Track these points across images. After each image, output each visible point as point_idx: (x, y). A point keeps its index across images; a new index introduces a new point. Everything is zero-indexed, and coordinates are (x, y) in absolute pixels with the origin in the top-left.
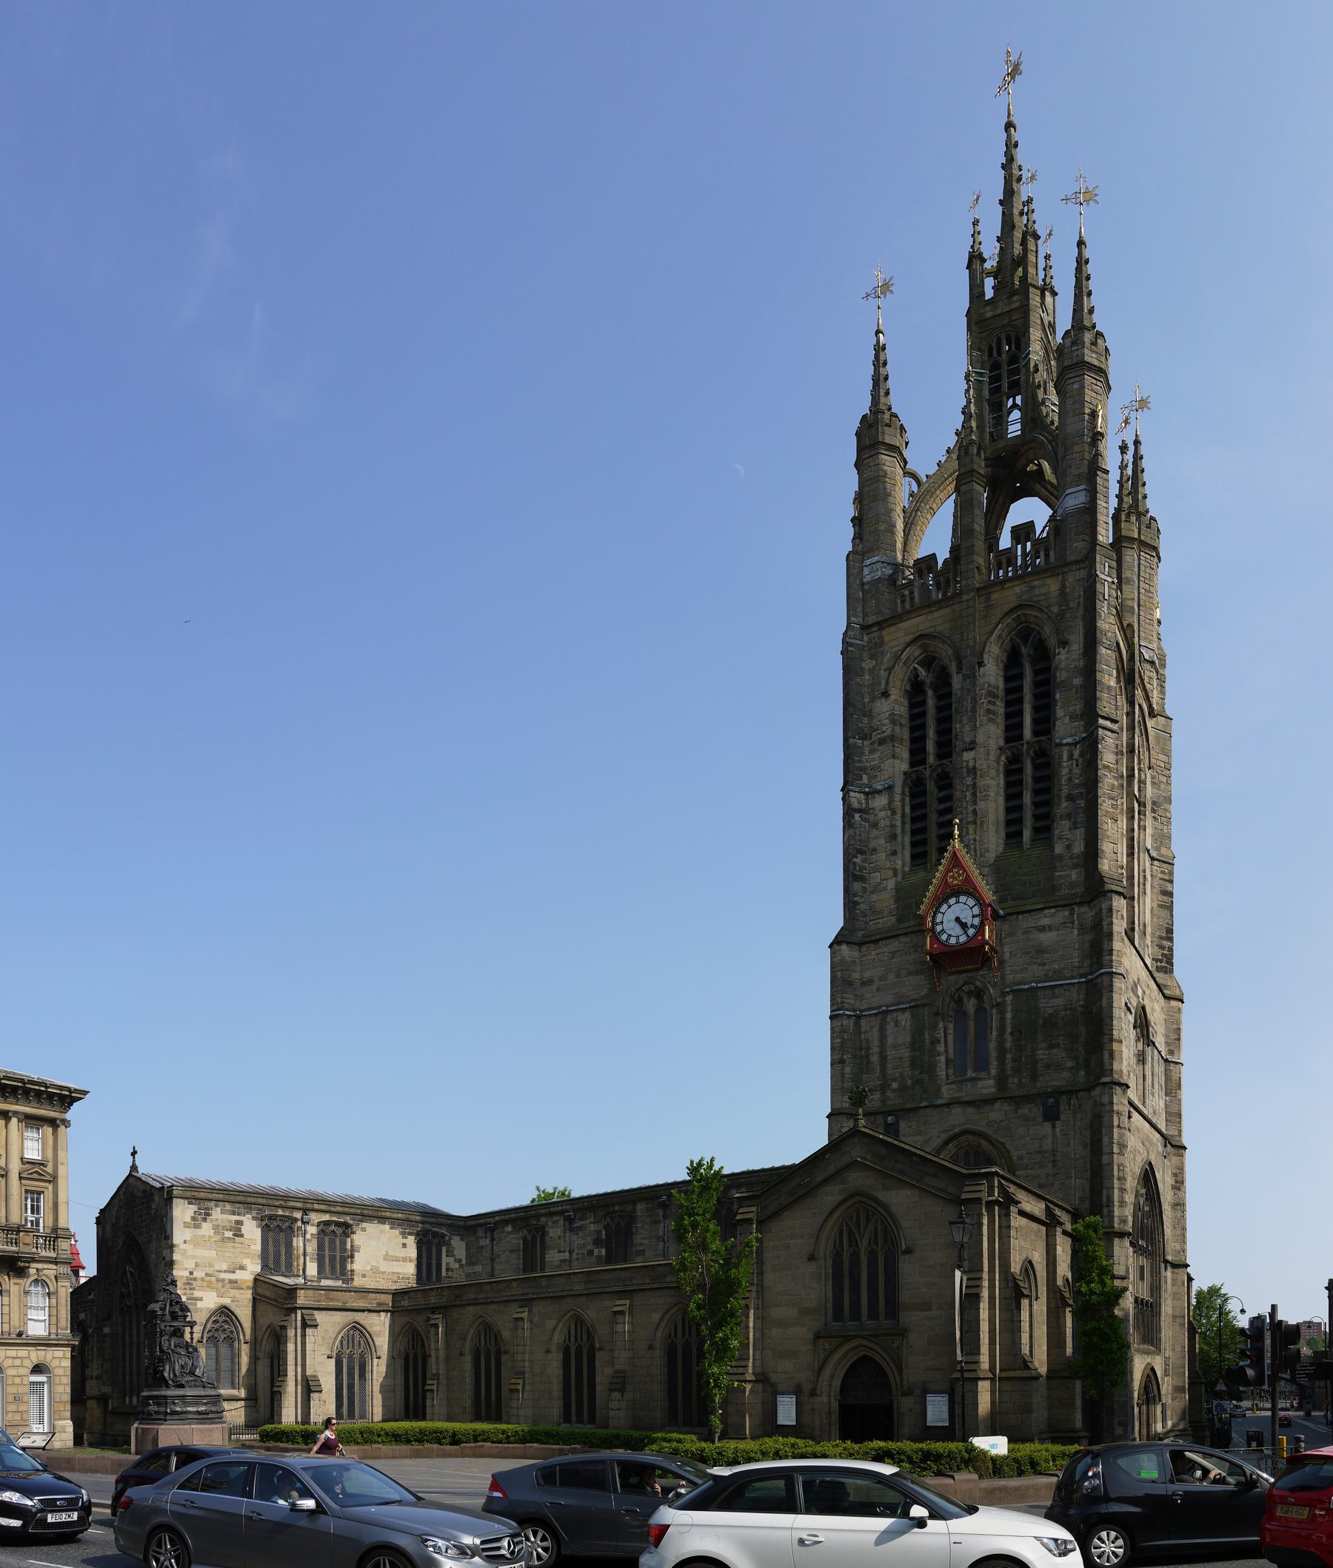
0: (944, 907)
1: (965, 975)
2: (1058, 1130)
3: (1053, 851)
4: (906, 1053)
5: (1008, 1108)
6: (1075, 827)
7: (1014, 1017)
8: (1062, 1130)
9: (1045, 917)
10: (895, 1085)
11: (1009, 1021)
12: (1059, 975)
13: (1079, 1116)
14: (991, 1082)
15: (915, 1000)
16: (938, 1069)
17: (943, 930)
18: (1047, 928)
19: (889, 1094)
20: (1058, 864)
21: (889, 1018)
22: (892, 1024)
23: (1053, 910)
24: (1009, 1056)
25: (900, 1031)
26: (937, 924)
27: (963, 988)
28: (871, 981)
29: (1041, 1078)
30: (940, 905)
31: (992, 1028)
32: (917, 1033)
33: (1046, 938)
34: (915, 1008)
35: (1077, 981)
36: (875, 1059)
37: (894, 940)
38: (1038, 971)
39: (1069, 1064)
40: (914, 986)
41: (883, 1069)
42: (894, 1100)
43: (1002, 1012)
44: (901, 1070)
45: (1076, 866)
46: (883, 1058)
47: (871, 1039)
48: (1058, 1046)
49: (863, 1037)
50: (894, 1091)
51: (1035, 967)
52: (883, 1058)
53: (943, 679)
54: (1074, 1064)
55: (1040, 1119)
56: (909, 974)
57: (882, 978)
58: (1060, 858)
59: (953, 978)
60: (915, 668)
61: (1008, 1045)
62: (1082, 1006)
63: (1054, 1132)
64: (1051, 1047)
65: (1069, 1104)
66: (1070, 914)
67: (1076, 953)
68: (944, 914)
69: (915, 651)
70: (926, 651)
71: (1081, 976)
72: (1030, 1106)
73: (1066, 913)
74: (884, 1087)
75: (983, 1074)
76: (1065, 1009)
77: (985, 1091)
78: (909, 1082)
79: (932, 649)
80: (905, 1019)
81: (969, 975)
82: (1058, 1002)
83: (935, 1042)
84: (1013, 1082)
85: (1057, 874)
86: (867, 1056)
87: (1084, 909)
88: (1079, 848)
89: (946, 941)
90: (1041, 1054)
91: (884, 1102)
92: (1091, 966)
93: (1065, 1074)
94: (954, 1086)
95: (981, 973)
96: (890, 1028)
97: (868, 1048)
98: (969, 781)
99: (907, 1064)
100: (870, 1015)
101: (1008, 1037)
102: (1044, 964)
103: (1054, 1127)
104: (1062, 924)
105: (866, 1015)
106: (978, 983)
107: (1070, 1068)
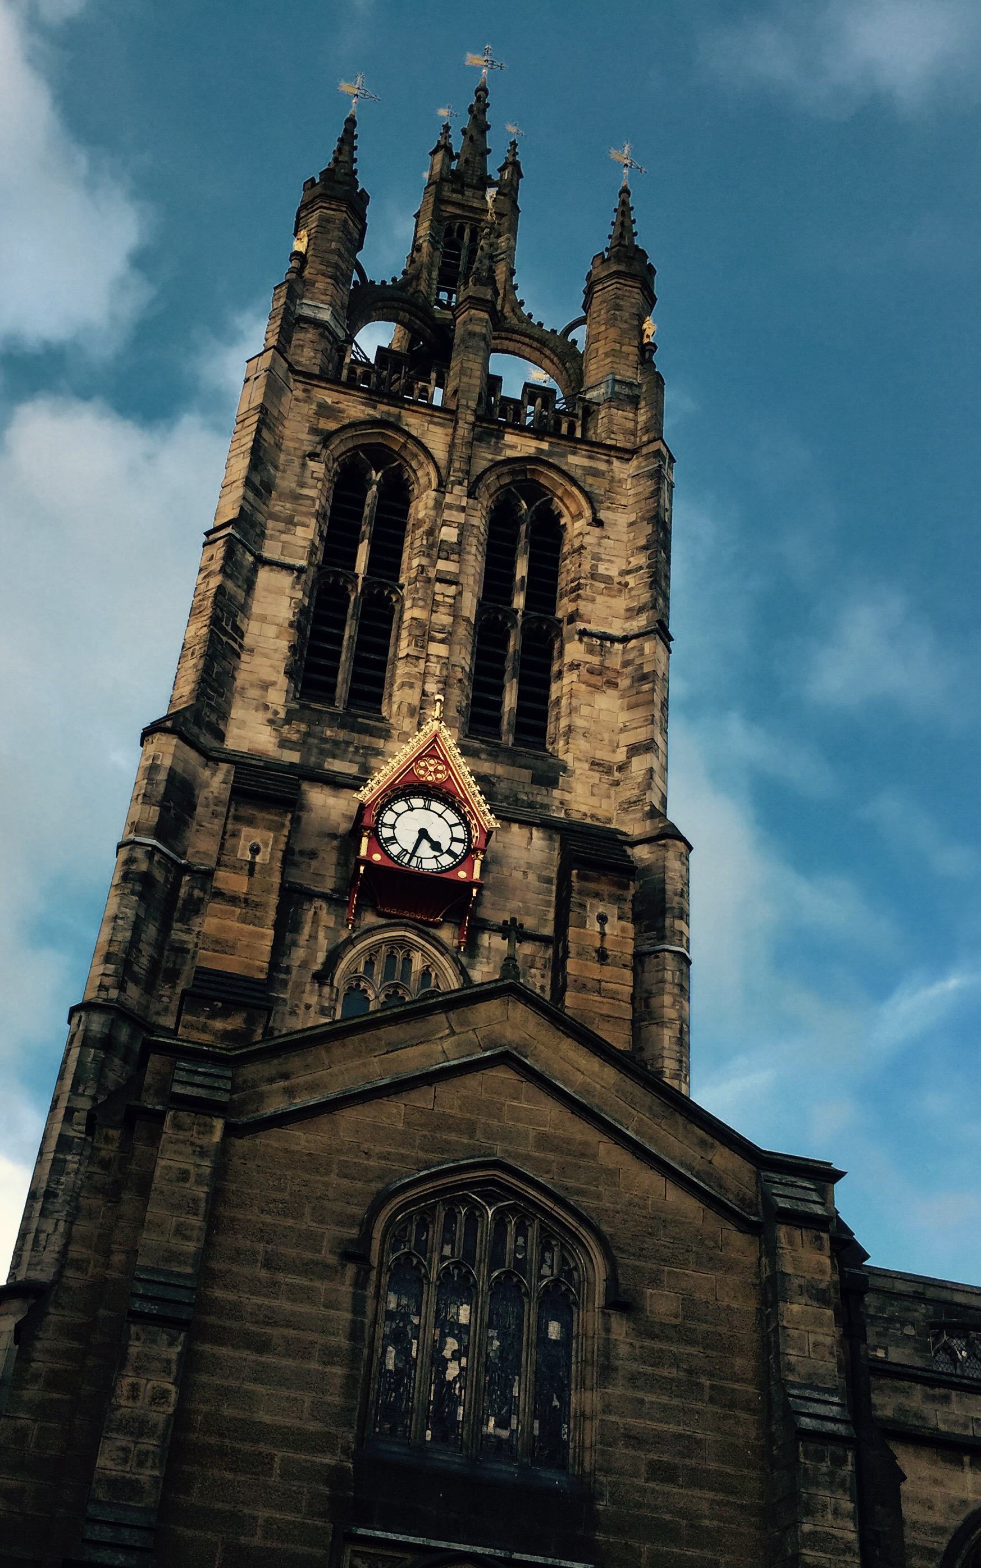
0: (400, 806)
17: (394, 838)
26: (384, 825)
30: (395, 799)
68: (399, 815)
89: (398, 857)
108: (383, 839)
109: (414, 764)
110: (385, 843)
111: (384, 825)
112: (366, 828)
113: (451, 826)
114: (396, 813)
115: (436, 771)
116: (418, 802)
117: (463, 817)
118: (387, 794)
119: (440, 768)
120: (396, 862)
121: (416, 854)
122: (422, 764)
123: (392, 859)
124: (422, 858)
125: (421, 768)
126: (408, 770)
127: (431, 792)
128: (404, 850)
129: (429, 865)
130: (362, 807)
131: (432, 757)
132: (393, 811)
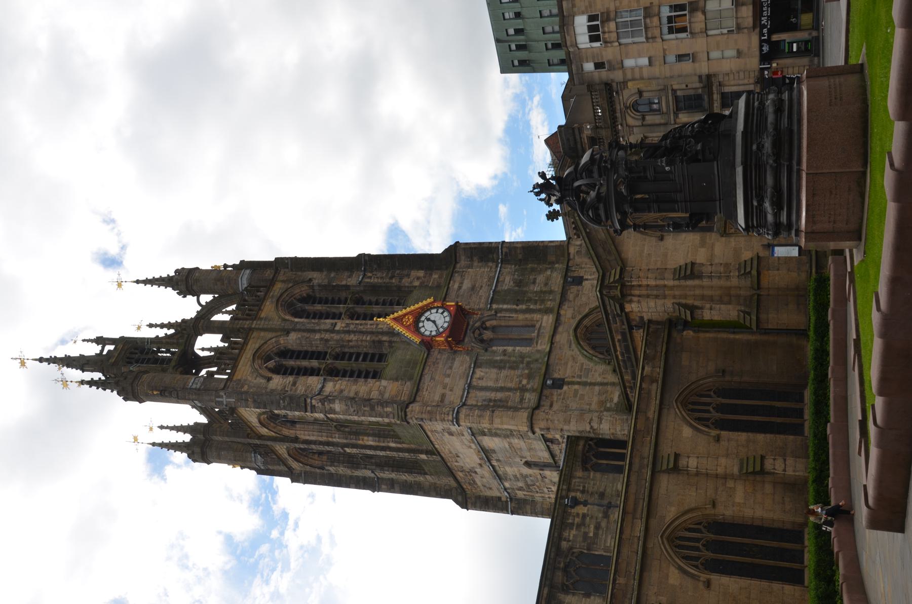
0: (422, 330)
1: (468, 331)
2: (589, 277)
3: (416, 287)
4: (504, 373)
5: (566, 306)
6: (408, 276)
7: (507, 304)
8: (591, 275)
10: (524, 382)
11: (509, 306)
12: (491, 279)
13: (583, 266)
14: (545, 317)
15: (470, 366)
16: (524, 352)
19: (529, 386)
21: (474, 383)
22: (480, 382)
23: (451, 282)
24: (532, 307)
25: (487, 376)
28: (443, 396)
29: (552, 288)
31: (509, 317)
32: (493, 364)
33: (467, 284)
34: (477, 364)
35: (499, 269)
36: (499, 395)
37: (423, 378)
38: (485, 288)
39: (549, 273)
40: (461, 363)
41: (510, 390)
42: (536, 383)
43: (501, 310)
44: (515, 377)
45: (431, 275)
46: (502, 389)
47: (484, 398)
48: (535, 279)
49: (479, 404)
50: (528, 383)
51: (481, 291)
52: (502, 389)
53: (285, 353)
54: (550, 270)
55: (580, 287)
56: (451, 368)
57: (445, 387)
58: (421, 283)
59: (466, 340)
60: (266, 367)
61: (524, 307)
62: (515, 266)
63: (590, 280)
64: (534, 283)
65: (575, 271)
67: (482, 270)
69: (258, 362)
70: (262, 359)
71: (497, 267)
72: (569, 293)
73: (456, 275)
74: (523, 390)
75: (538, 326)
76: (514, 275)
77: (551, 320)
78: (526, 371)
79: (264, 354)
80: (479, 373)
81: (470, 327)
82: (508, 279)
83: (504, 353)
84: (549, 304)
86: (495, 401)
87: (458, 265)
88: (421, 273)
90: (536, 288)
91: (533, 390)
92: (493, 261)
93: (555, 274)
94: (539, 342)
95: (471, 323)
96: (482, 383)
97: (490, 400)
99: (512, 372)
100: (466, 397)
101: (520, 307)
102: (482, 286)
103: (587, 280)
105: (465, 400)
106: (477, 324)
107: (552, 272)
111: (430, 334)
115: (408, 318)
116: (421, 325)
117: (428, 310)
126: (407, 328)
127: (417, 320)
129: (448, 319)
131: (402, 320)
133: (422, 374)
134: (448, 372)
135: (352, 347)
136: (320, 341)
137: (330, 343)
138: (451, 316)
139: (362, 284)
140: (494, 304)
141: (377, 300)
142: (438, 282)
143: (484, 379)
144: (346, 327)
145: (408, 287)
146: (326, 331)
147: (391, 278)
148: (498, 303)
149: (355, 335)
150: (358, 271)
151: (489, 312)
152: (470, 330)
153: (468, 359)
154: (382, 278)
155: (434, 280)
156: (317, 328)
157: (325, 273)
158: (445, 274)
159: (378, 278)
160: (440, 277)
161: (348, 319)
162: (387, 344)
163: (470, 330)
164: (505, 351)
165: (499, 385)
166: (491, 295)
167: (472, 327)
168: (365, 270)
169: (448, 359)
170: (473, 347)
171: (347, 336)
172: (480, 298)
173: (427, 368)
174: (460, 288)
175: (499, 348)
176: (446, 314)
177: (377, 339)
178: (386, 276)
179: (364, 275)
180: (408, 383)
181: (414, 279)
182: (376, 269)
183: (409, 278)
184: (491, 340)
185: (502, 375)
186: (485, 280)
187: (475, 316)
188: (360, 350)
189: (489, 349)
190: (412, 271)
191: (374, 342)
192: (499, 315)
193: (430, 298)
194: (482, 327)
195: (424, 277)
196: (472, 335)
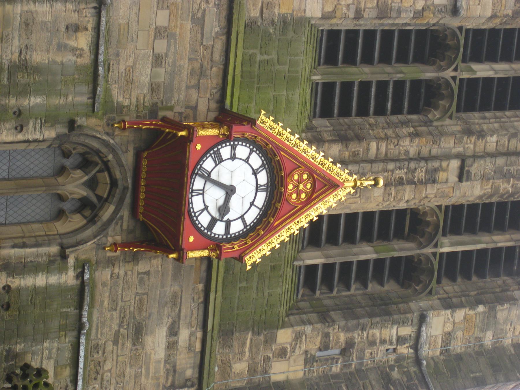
0: (256, 161)
7: (36, 290)
9: (192, 334)
17: (221, 161)
18: (173, 339)
20: (262, 338)
22: (74, 18)
23: (198, 347)
27: (106, 173)
31: (24, 246)
37: (224, 23)
45: (252, 370)
51: (115, 327)
58: (270, 340)
66: (187, 380)
68: (247, 161)
85: (250, 336)
95: (125, 213)
98: (420, 174)
102: (116, 342)
104: (174, 367)
108: (218, 150)
109: (303, 168)
110: (214, 152)
111: (234, 148)
112: (230, 129)
113: (242, 217)
114: (248, 158)
115: (299, 193)
116: (263, 178)
118: (267, 144)
119: (303, 196)
120: (195, 168)
121: (209, 185)
122: (305, 177)
123: (198, 163)
124: (203, 194)
125: (300, 176)
128: (210, 173)
129: (197, 203)
130: (252, 122)
132: (250, 154)
133: (229, 34)
134: (161, 46)
135: (405, 123)
136: (483, 130)
137: (458, 128)
138: (189, 213)
139: (416, 314)
140: (71, 288)
141: (366, 287)
142: (231, 346)
143: (63, 28)
144: (436, 170)
145: (304, 323)
146: (475, 157)
147: (350, 345)
148: (61, 289)
149: (407, 152)
150: (433, 358)
151: (83, 257)
152: (126, 188)
153: (115, 92)
154: (372, 343)
155: (242, 353)
156: (500, 161)
157: (507, 342)
158: (218, 377)
159: (383, 342)
160: (226, 366)
161: (425, 213)
162: (326, 136)
163: (126, 188)
164: (20, 128)
165: (18, 8)
166: (85, 313)
167: (121, 200)
168: (418, 361)
169: (169, 88)
170: (108, 134)
171: (425, 151)
172: (113, 300)
173: (218, 56)
174: (173, 332)
175: (38, 136)
176: (204, 220)
177: (354, 147)
178: (363, 351)
179: (416, 347)
180: (255, 13)
181: (293, 350)
182: (392, 368)
183: (306, 352)
184: (62, 171)
185: (16, 42)
186: (108, 366)
187: (118, 239)
188: (381, 119)
189: (62, 129)
190: (300, 375)
191: (360, 139)
192: (54, 249)
193: (254, 265)
194: (93, 207)
195: (266, 360)
196: (118, 175)
